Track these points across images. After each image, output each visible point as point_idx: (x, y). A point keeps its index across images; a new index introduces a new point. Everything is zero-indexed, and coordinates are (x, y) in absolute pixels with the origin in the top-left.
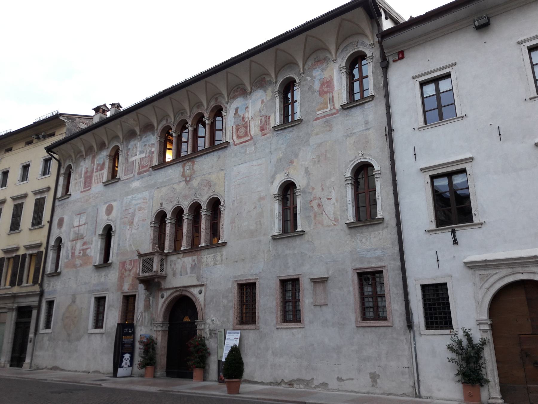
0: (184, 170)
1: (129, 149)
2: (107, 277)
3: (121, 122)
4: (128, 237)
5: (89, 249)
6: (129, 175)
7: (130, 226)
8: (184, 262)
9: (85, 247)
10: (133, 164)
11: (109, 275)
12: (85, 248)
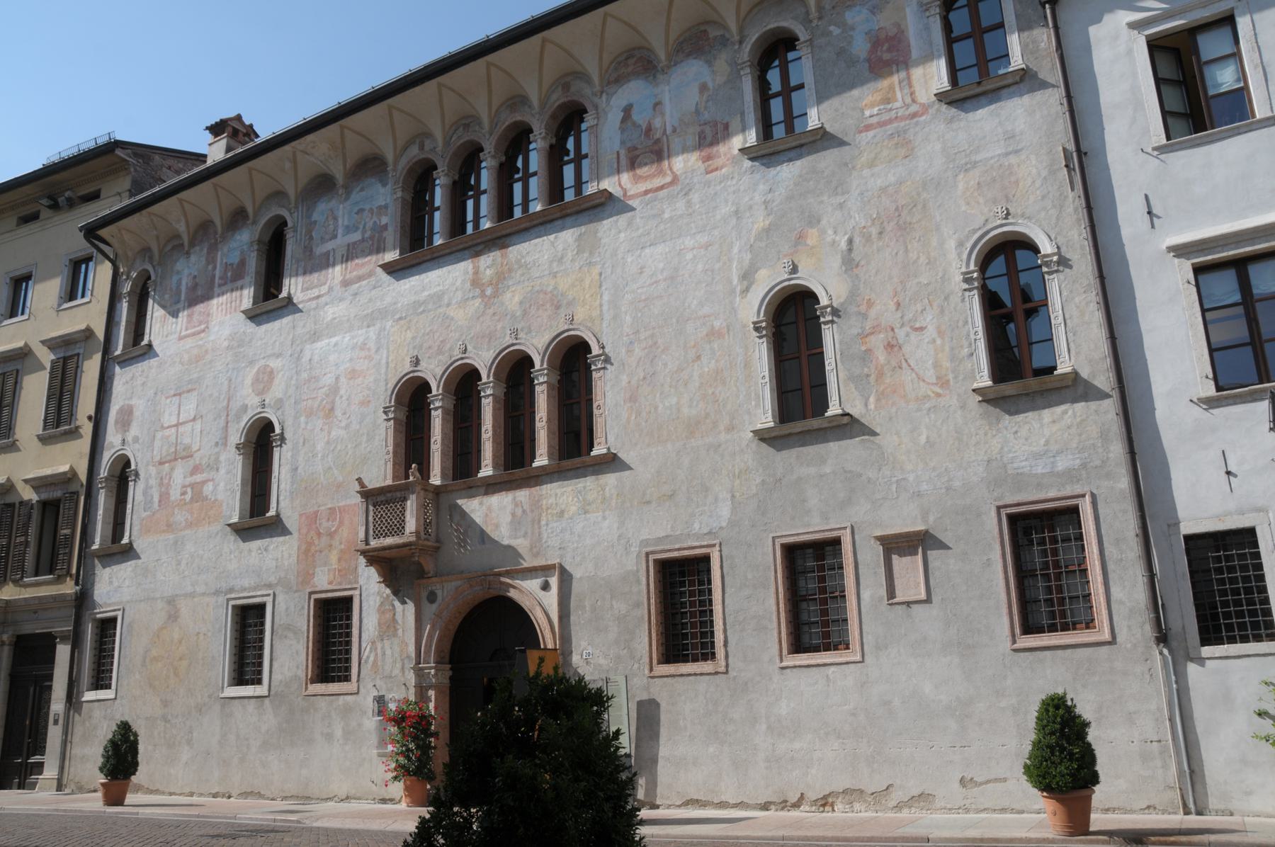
1: (315, 222)
3: (294, 153)
5: (210, 484)
6: (314, 290)
8: (489, 509)
9: (198, 478)
10: (328, 259)
12: (198, 480)
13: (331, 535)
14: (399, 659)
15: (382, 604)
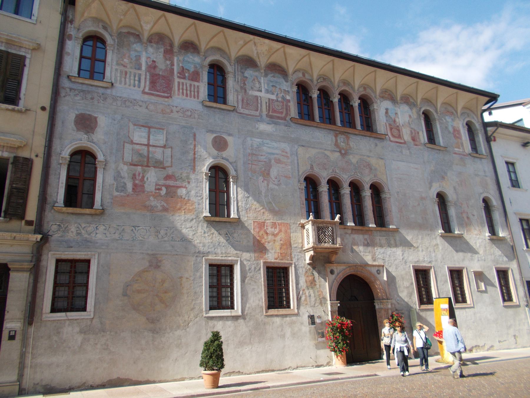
0: (336, 141)
1: (247, 77)
4: (263, 191)
6: (250, 111)
7: (263, 177)
8: (354, 239)
9: (171, 183)
10: (257, 100)
11: (235, 235)
13: (275, 235)
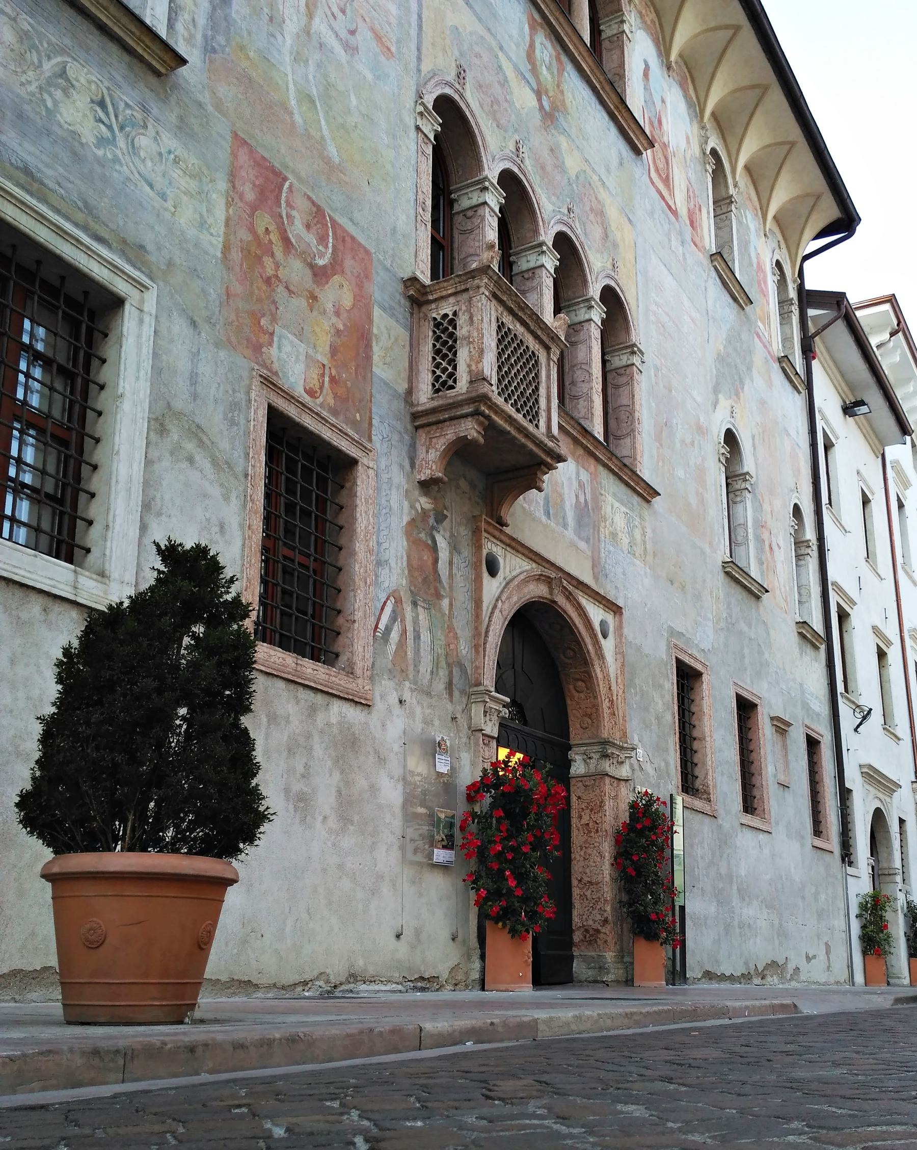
2: (121, 142)
14: (443, 664)
15: (412, 523)
